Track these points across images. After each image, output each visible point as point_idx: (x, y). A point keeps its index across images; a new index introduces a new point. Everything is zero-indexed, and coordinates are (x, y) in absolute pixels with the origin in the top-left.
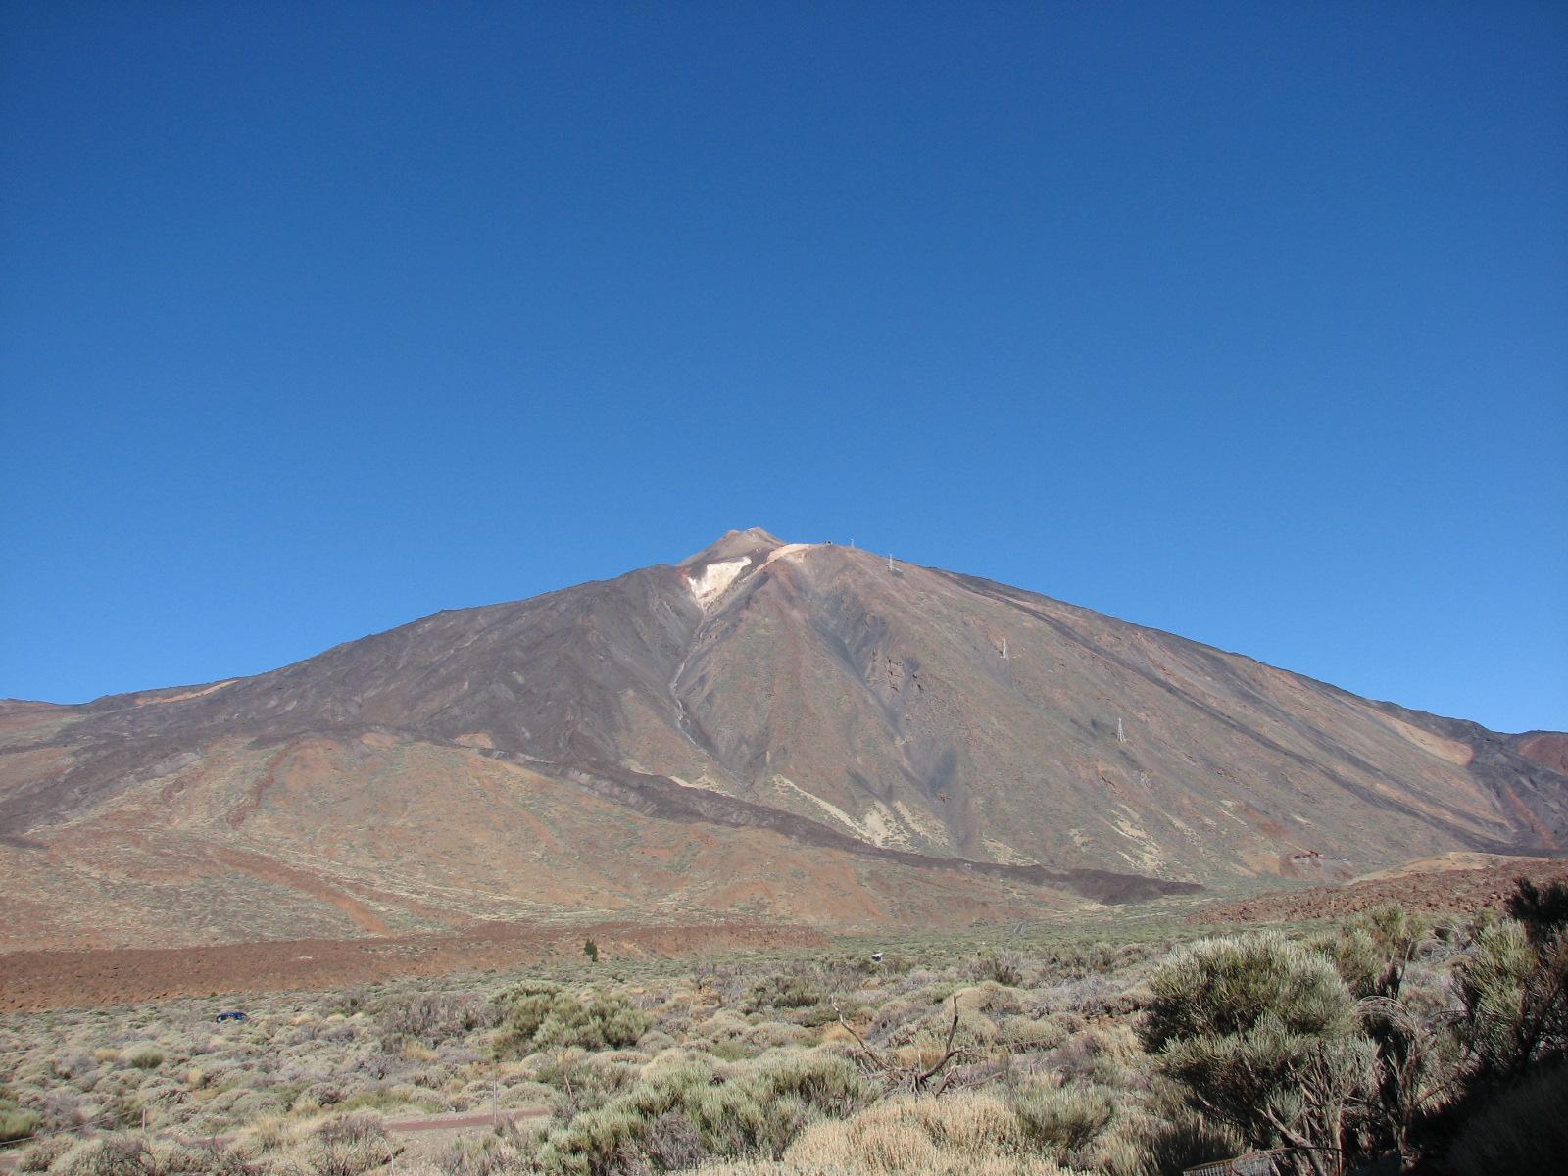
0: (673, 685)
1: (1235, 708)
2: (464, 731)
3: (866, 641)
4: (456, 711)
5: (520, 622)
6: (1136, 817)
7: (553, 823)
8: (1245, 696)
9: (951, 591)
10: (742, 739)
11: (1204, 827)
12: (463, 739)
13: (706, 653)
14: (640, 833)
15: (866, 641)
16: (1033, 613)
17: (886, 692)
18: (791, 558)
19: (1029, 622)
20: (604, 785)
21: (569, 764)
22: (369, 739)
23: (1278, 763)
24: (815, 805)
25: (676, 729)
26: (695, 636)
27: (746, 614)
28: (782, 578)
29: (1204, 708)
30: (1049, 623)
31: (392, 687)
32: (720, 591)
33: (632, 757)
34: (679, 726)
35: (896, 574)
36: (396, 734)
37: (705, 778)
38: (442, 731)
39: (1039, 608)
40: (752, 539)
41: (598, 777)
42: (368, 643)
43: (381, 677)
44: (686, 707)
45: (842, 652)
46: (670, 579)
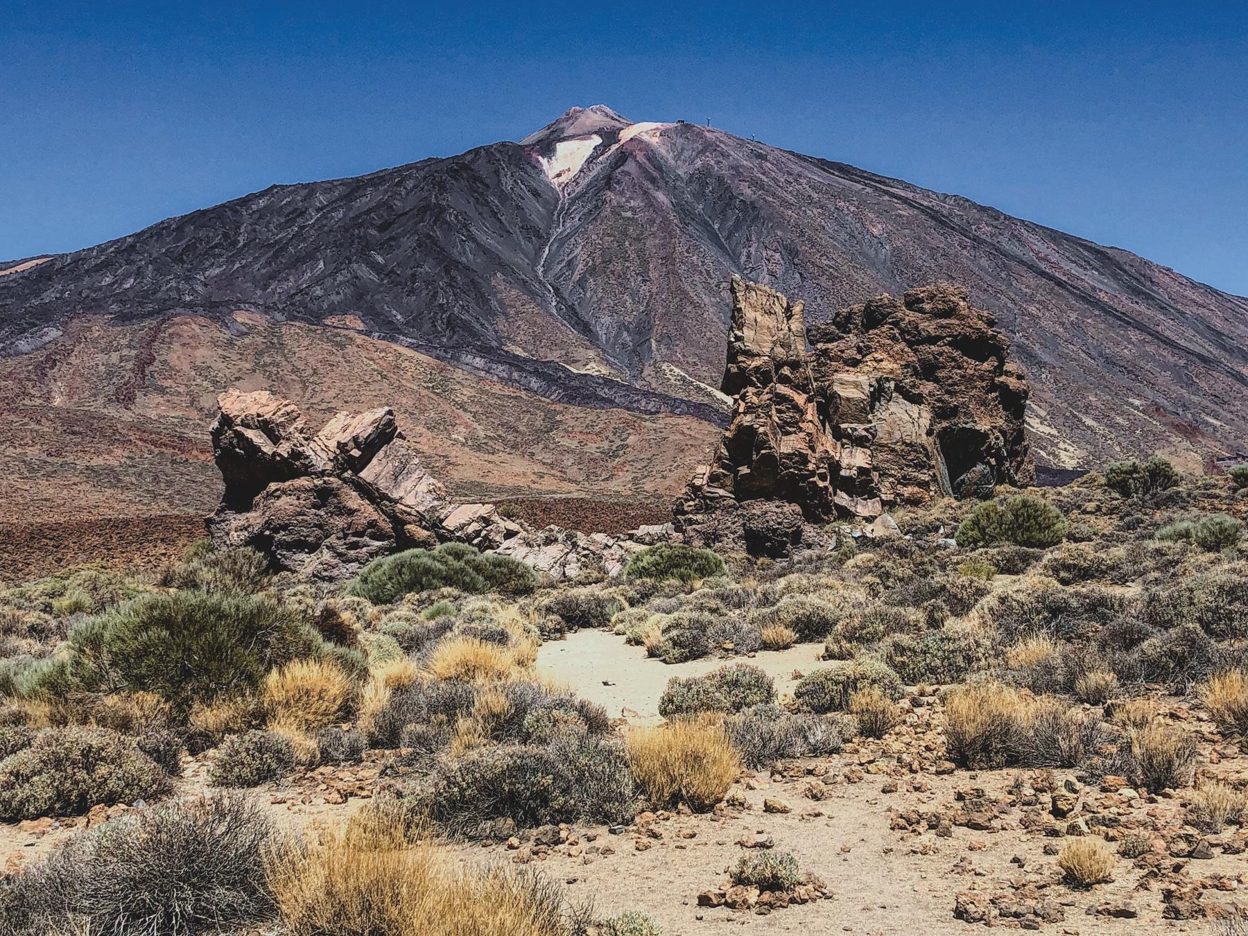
0: (540, 270)
1: (1126, 303)
2: (332, 311)
3: (737, 226)
4: (319, 292)
5: (364, 199)
6: (1043, 413)
7: (462, 406)
8: (1136, 292)
9: (817, 176)
10: (623, 326)
11: (1113, 426)
12: (328, 322)
13: (569, 236)
14: (558, 418)
15: (737, 226)
16: (905, 200)
18: (645, 137)
19: (905, 211)
20: (501, 370)
21: (458, 347)
22: (241, 317)
23: (1182, 362)
24: (709, 395)
25: (551, 315)
26: (555, 217)
27: (609, 195)
28: (640, 157)
30: (923, 211)
31: (237, 265)
32: (576, 170)
33: (514, 342)
34: (554, 311)
35: (759, 156)
36: (266, 313)
37: (593, 364)
38: (310, 313)
39: (910, 195)
40: (594, 117)
41: (492, 361)
42: (199, 218)
43: (221, 255)
44: (557, 291)
45: (714, 238)
46: (522, 158)
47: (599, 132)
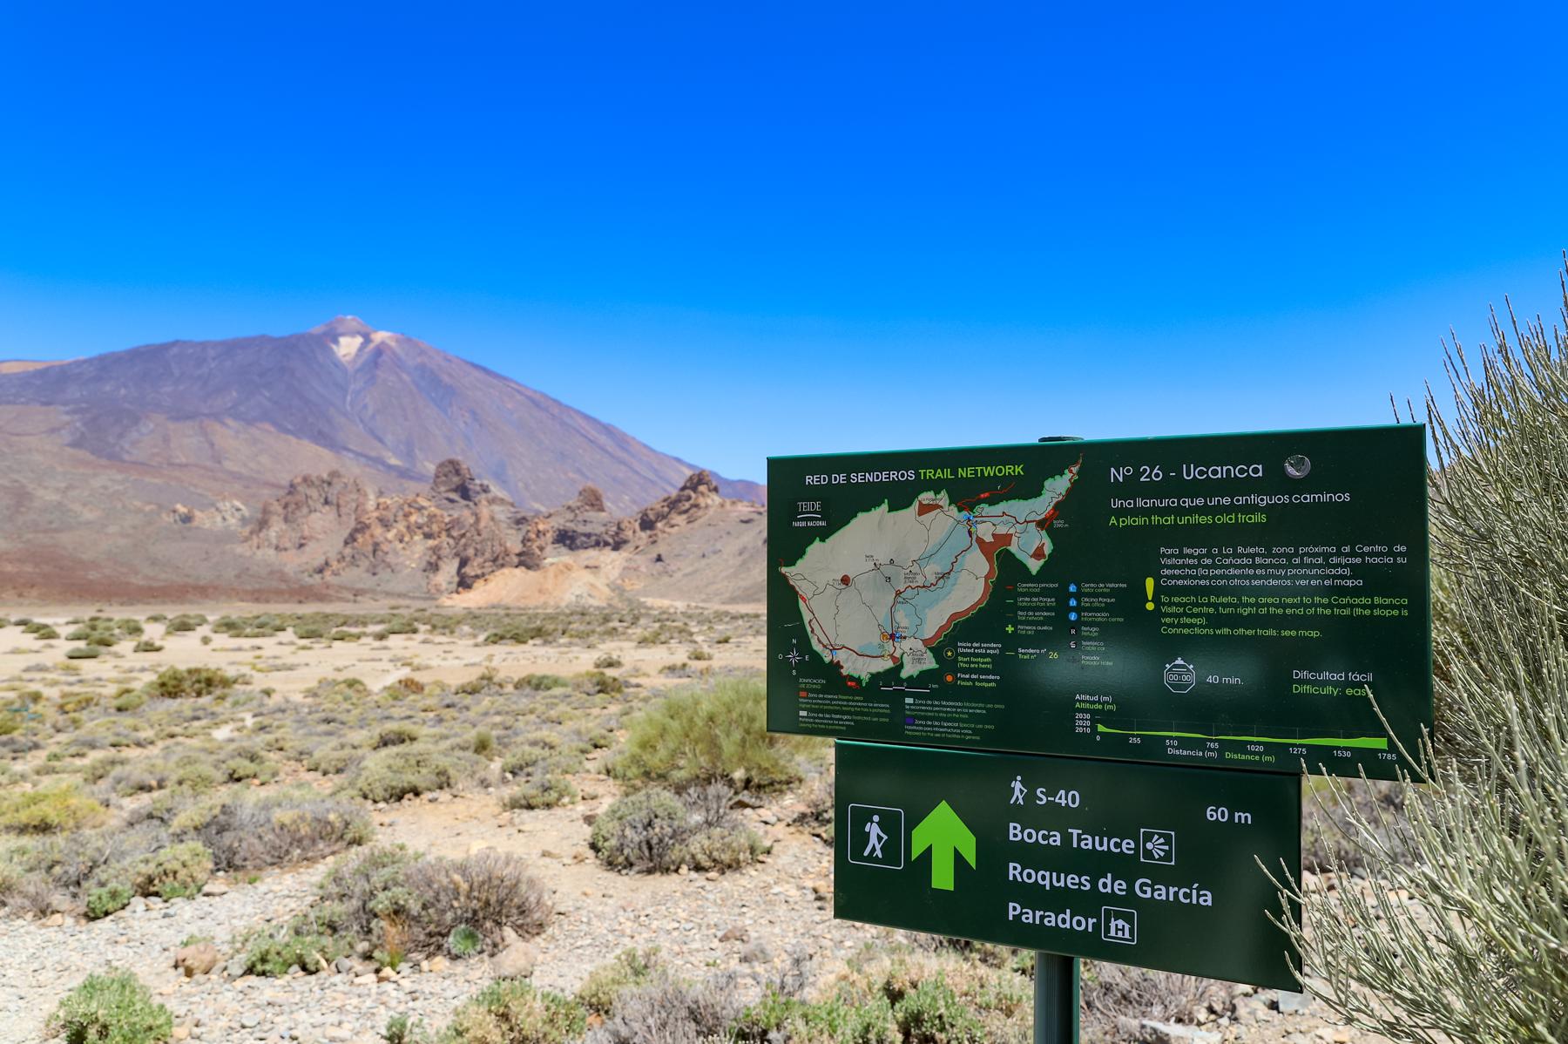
9: (477, 374)
17: (462, 425)
19: (519, 397)
27: (379, 373)
29: (607, 452)
47: (359, 333)
